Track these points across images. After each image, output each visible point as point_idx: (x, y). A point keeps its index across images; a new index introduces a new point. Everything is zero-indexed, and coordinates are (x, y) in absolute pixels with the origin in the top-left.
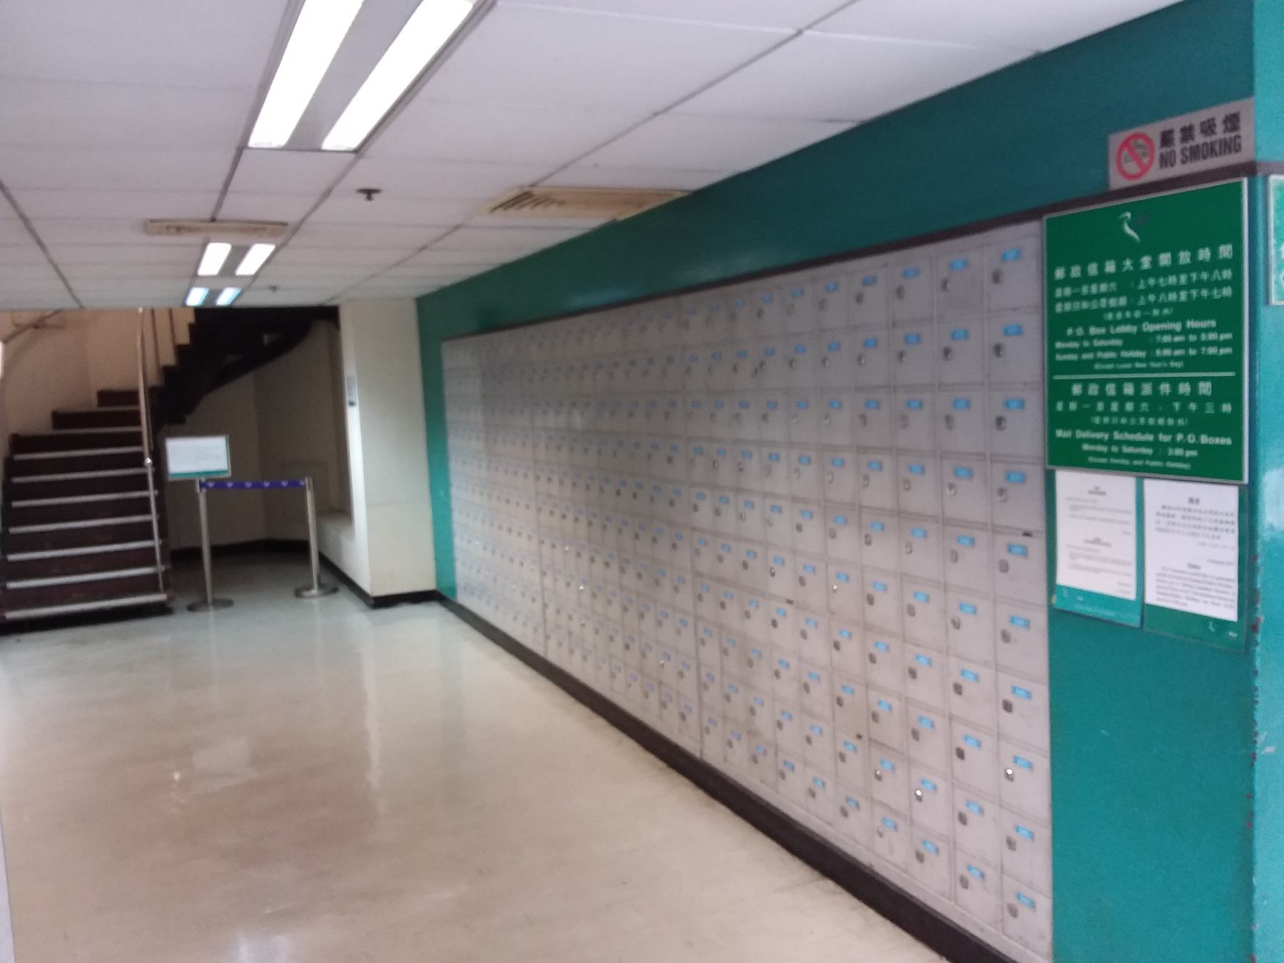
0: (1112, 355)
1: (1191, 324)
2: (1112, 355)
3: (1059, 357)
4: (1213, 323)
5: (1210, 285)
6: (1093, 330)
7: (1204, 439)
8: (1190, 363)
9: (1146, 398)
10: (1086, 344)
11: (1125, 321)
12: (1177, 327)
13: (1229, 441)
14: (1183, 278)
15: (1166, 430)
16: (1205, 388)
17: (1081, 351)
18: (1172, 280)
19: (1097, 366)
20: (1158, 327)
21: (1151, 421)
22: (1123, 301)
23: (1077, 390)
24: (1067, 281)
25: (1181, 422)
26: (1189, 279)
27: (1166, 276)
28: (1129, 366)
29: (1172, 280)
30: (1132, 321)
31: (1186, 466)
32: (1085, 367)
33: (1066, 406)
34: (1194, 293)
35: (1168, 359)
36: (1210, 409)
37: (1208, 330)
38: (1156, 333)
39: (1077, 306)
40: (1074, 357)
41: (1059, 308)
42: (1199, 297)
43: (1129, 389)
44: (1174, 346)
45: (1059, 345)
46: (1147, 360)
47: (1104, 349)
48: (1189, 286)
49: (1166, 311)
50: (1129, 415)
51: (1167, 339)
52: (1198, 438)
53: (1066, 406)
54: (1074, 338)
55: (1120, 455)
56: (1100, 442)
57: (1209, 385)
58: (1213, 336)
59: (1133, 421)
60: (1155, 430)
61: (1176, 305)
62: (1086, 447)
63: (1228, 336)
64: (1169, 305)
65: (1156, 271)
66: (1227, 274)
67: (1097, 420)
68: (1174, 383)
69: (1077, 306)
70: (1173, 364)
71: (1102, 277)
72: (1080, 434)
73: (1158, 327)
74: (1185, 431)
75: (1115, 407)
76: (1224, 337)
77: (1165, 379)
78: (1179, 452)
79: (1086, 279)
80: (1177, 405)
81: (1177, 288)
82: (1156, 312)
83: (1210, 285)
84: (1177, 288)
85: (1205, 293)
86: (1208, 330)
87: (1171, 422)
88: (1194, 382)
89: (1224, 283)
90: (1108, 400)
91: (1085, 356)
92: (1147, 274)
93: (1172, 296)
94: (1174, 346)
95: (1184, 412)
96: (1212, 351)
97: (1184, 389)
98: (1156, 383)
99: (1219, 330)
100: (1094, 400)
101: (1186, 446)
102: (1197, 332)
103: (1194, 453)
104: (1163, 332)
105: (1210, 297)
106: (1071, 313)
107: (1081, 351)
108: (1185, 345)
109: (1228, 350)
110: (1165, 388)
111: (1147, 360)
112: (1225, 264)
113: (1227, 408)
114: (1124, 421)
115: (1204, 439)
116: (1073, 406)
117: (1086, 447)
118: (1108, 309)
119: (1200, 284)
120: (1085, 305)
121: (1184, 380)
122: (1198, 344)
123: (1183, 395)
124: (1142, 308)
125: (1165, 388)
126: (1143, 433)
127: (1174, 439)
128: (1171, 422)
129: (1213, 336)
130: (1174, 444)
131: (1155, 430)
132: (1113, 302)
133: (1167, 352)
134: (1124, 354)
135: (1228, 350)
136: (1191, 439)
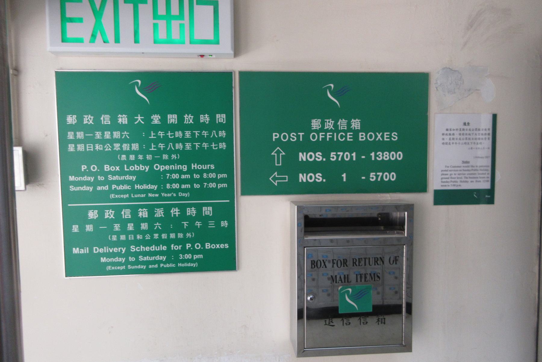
0: (127, 187)
1: (194, 166)
2: (127, 187)
3: (72, 188)
4: (213, 167)
5: (209, 140)
6: (107, 168)
7: (208, 246)
8: (195, 194)
9: (159, 220)
10: (101, 178)
11: (137, 162)
12: (185, 168)
13: (227, 246)
14: (188, 134)
15: (177, 241)
16: (208, 211)
17: (96, 183)
18: (178, 134)
19: (112, 196)
20: (167, 167)
21: (164, 236)
22: (135, 147)
23: (92, 215)
24: (79, 126)
25: (188, 235)
26: (193, 135)
27: (173, 131)
28: (143, 196)
29: (178, 134)
30: (145, 162)
31: (194, 265)
32: (104, 196)
33: (82, 228)
34: (197, 145)
35: (176, 191)
36: (212, 224)
37: (208, 171)
38: (165, 171)
39: (90, 147)
40: (91, 189)
41: (71, 148)
42: (201, 148)
43: (143, 213)
44: (181, 181)
45: (72, 178)
46: (158, 191)
47: (118, 183)
48: (193, 140)
49: (174, 156)
50: (144, 233)
51: (176, 176)
52: (203, 245)
53: (82, 228)
54: (90, 173)
55: (137, 262)
56: (119, 255)
57: (210, 208)
58: (212, 175)
59: (148, 237)
60: (168, 242)
61: (183, 153)
62: (103, 260)
63: (225, 176)
64: (177, 152)
65: (164, 126)
66: (222, 134)
67: (114, 238)
68: (184, 208)
69: (90, 147)
70: (180, 194)
71: (114, 126)
72: (97, 250)
73: (167, 167)
74: (192, 241)
75: (130, 227)
76: (220, 176)
77: (175, 206)
78: (188, 256)
79: (98, 126)
80: (185, 224)
81: (183, 140)
82: (165, 157)
83: (209, 140)
84: (183, 140)
85: (205, 145)
86: (208, 171)
87: (180, 235)
88: (199, 208)
89: (221, 140)
90: (124, 223)
91: (99, 188)
92: (156, 128)
93: (179, 146)
94: (181, 181)
95: (191, 228)
96: (212, 185)
97: (191, 212)
98: (167, 209)
99: (217, 171)
100: (110, 222)
101: (193, 252)
102: (201, 172)
103: (201, 256)
104: (171, 172)
105: (210, 148)
106: (85, 153)
107: (96, 183)
108: (191, 181)
109: (225, 185)
110: (175, 212)
111: (158, 191)
112: (221, 127)
113: (224, 224)
114: (139, 237)
115: (208, 246)
116: (89, 228)
117: (103, 260)
118: (121, 152)
119: (201, 139)
120: (98, 147)
121: (190, 206)
122: (201, 181)
123: (191, 216)
124: (152, 153)
125: (175, 212)
126: (157, 245)
127: (184, 247)
128: (180, 235)
129: (212, 175)
130: (184, 251)
131: (168, 242)
132: (126, 147)
133: (176, 186)
134: (138, 187)
135: (225, 185)
136: (198, 246)
